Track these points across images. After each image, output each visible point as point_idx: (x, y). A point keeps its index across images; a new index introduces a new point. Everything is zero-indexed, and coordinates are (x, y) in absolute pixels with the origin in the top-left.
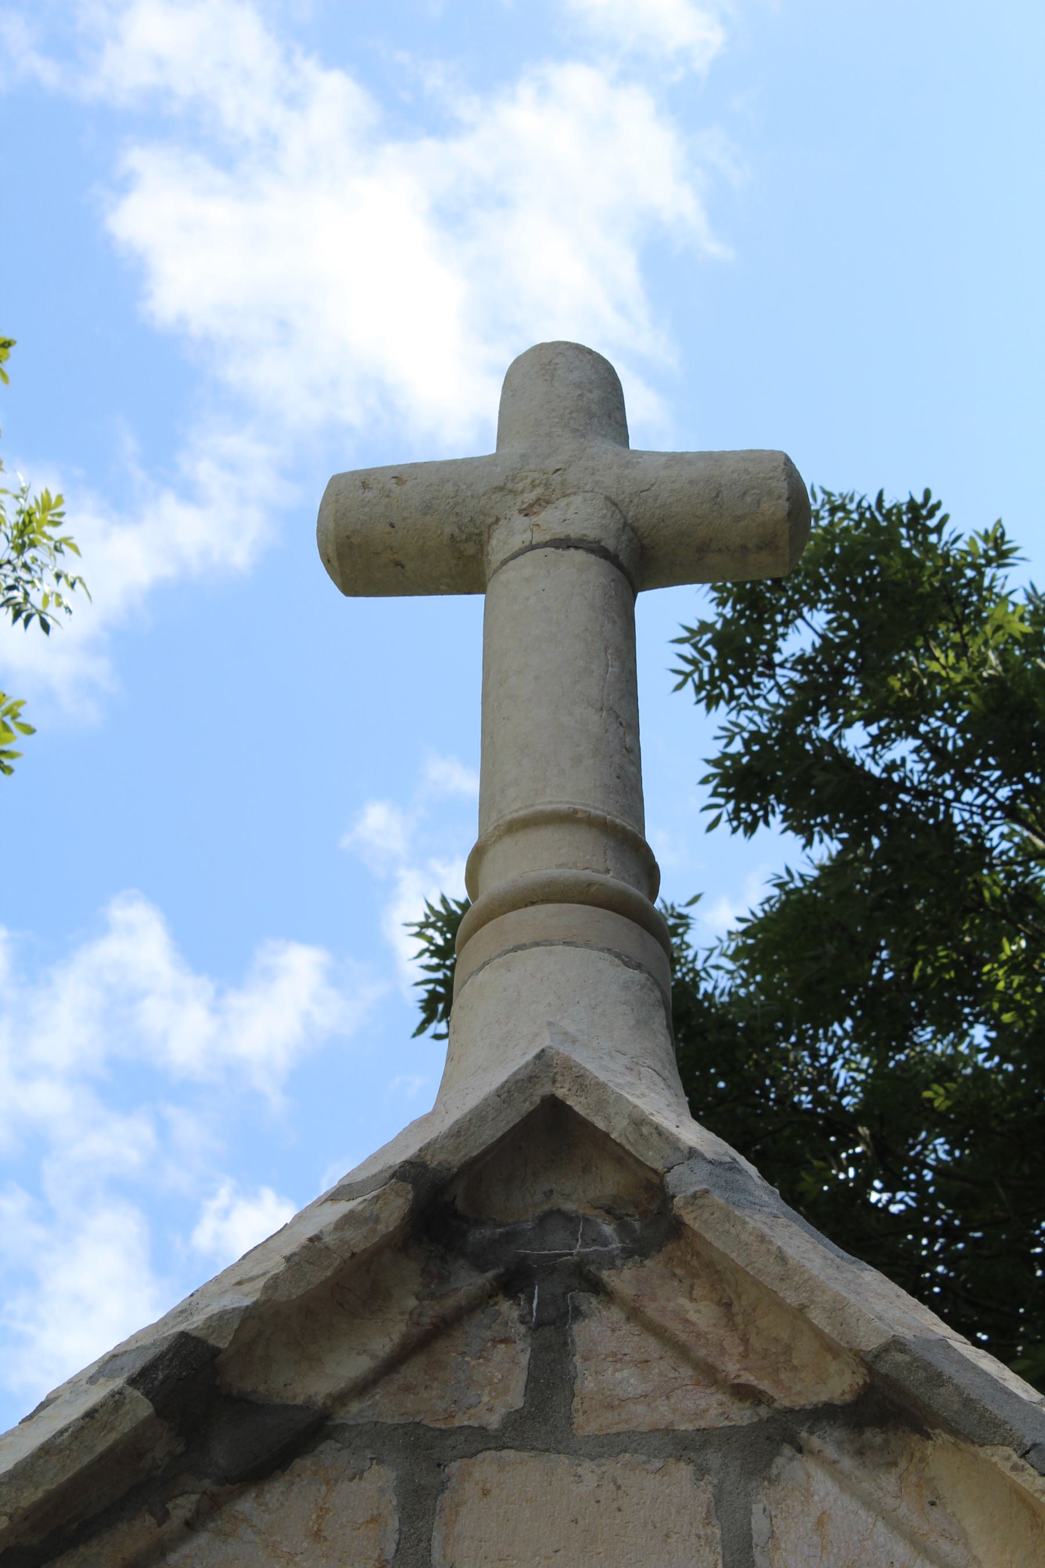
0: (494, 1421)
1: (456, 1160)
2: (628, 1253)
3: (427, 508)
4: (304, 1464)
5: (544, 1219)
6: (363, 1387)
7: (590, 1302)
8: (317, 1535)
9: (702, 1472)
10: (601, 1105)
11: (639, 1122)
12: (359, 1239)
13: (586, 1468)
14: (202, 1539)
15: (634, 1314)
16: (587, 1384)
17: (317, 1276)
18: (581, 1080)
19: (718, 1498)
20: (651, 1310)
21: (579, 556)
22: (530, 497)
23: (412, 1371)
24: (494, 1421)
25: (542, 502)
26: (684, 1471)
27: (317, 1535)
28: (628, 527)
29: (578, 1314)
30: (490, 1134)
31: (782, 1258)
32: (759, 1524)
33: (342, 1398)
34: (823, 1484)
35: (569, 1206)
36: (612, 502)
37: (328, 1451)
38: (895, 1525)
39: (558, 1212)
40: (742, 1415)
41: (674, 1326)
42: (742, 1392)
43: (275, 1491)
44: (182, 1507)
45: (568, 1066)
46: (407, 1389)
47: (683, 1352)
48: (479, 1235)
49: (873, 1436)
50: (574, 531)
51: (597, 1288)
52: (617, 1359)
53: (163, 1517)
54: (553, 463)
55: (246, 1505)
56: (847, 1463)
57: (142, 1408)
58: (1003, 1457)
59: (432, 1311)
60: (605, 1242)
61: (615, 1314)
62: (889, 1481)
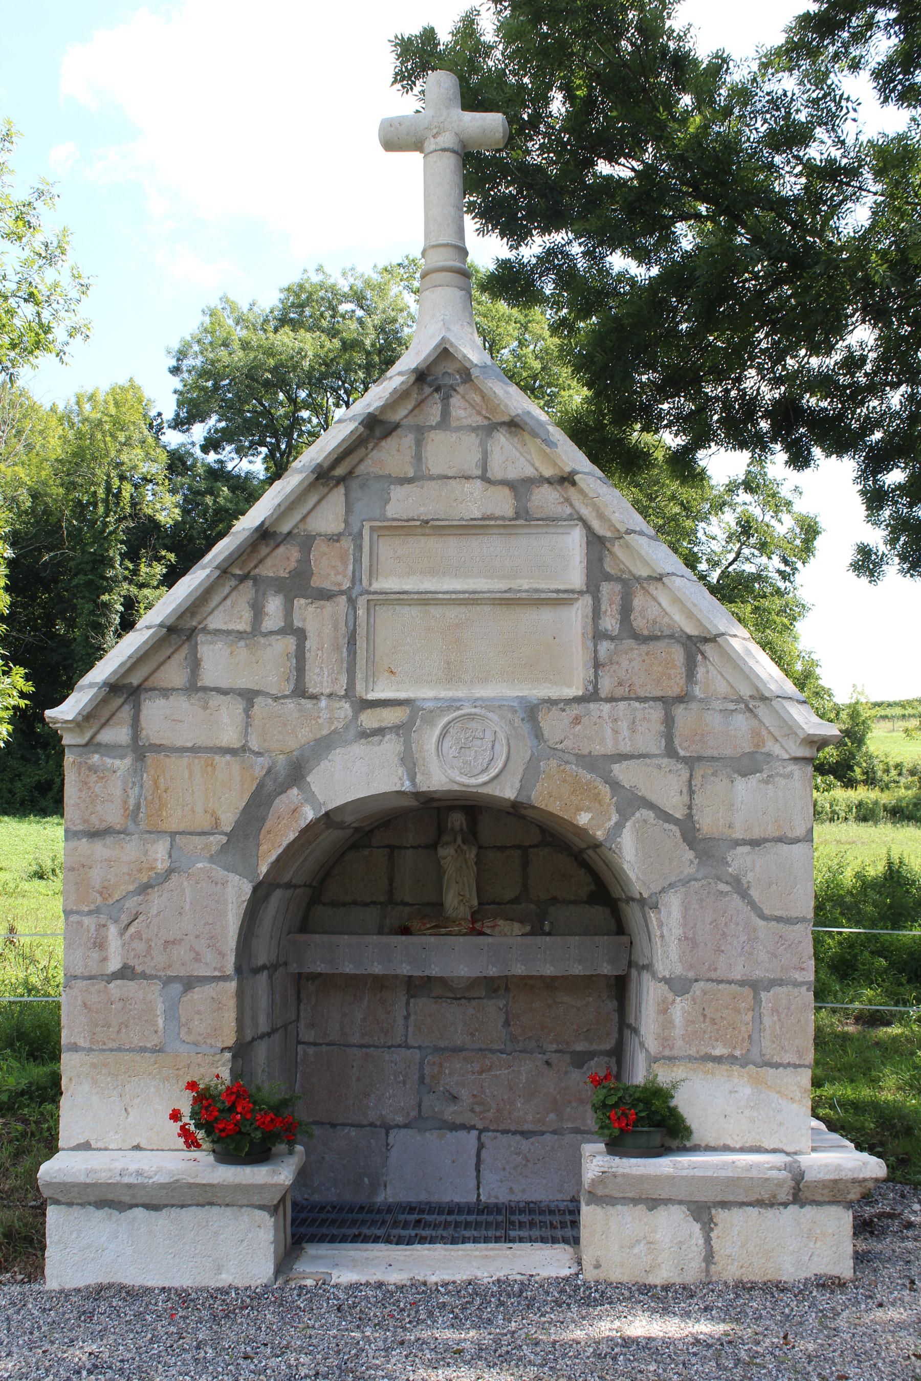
0: (434, 424)
1: (424, 366)
2: (462, 383)
3: (408, 134)
4: (394, 434)
5: (443, 374)
6: (406, 416)
7: (454, 393)
8: (398, 451)
9: (477, 435)
10: (456, 351)
11: (465, 356)
12: (404, 387)
13: (454, 435)
14: (375, 452)
15: (463, 397)
16: (454, 414)
17: (396, 396)
18: (452, 344)
19: (481, 440)
20: (467, 397)
21: (448, 154)
22: (435, 131)
23: (416, 411)
24: (434, 424)
25: (438, 133)
26: (474, 435)
27: (398, 451)
28: (461, 141)
29: (451, 396)
30: (431, 359)
31: (495, 393)
32: (489, 448)
33: (402, 419)
34: (503, 439)
35: (449, 371)
36: (456, 134)
37: (399, 430)
38: (517, 449)
39: (447, 372)
40: (486, 422)
41: (472, 402)
42: (486, 417)
43: (389, 440)
44: (370, 446)
45: (449, 340)
46: (415, 416)
47: (474, 407)
48: (430, 378)
49: (513, 429)
50: (447, 146)
51: (455, 390)
52: (460, 407)
53: (367, 448)
54: (441, 120)
55: (383, 443)
56: (507, 435)
57: (362, 429)
58: (539, 441)
59: (420, 398)
60: (456, 380)
61: (459, 397)
62: (516, 440)
